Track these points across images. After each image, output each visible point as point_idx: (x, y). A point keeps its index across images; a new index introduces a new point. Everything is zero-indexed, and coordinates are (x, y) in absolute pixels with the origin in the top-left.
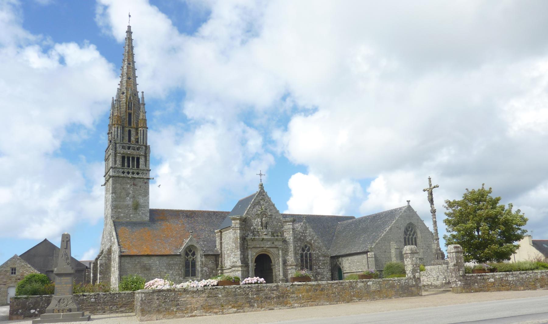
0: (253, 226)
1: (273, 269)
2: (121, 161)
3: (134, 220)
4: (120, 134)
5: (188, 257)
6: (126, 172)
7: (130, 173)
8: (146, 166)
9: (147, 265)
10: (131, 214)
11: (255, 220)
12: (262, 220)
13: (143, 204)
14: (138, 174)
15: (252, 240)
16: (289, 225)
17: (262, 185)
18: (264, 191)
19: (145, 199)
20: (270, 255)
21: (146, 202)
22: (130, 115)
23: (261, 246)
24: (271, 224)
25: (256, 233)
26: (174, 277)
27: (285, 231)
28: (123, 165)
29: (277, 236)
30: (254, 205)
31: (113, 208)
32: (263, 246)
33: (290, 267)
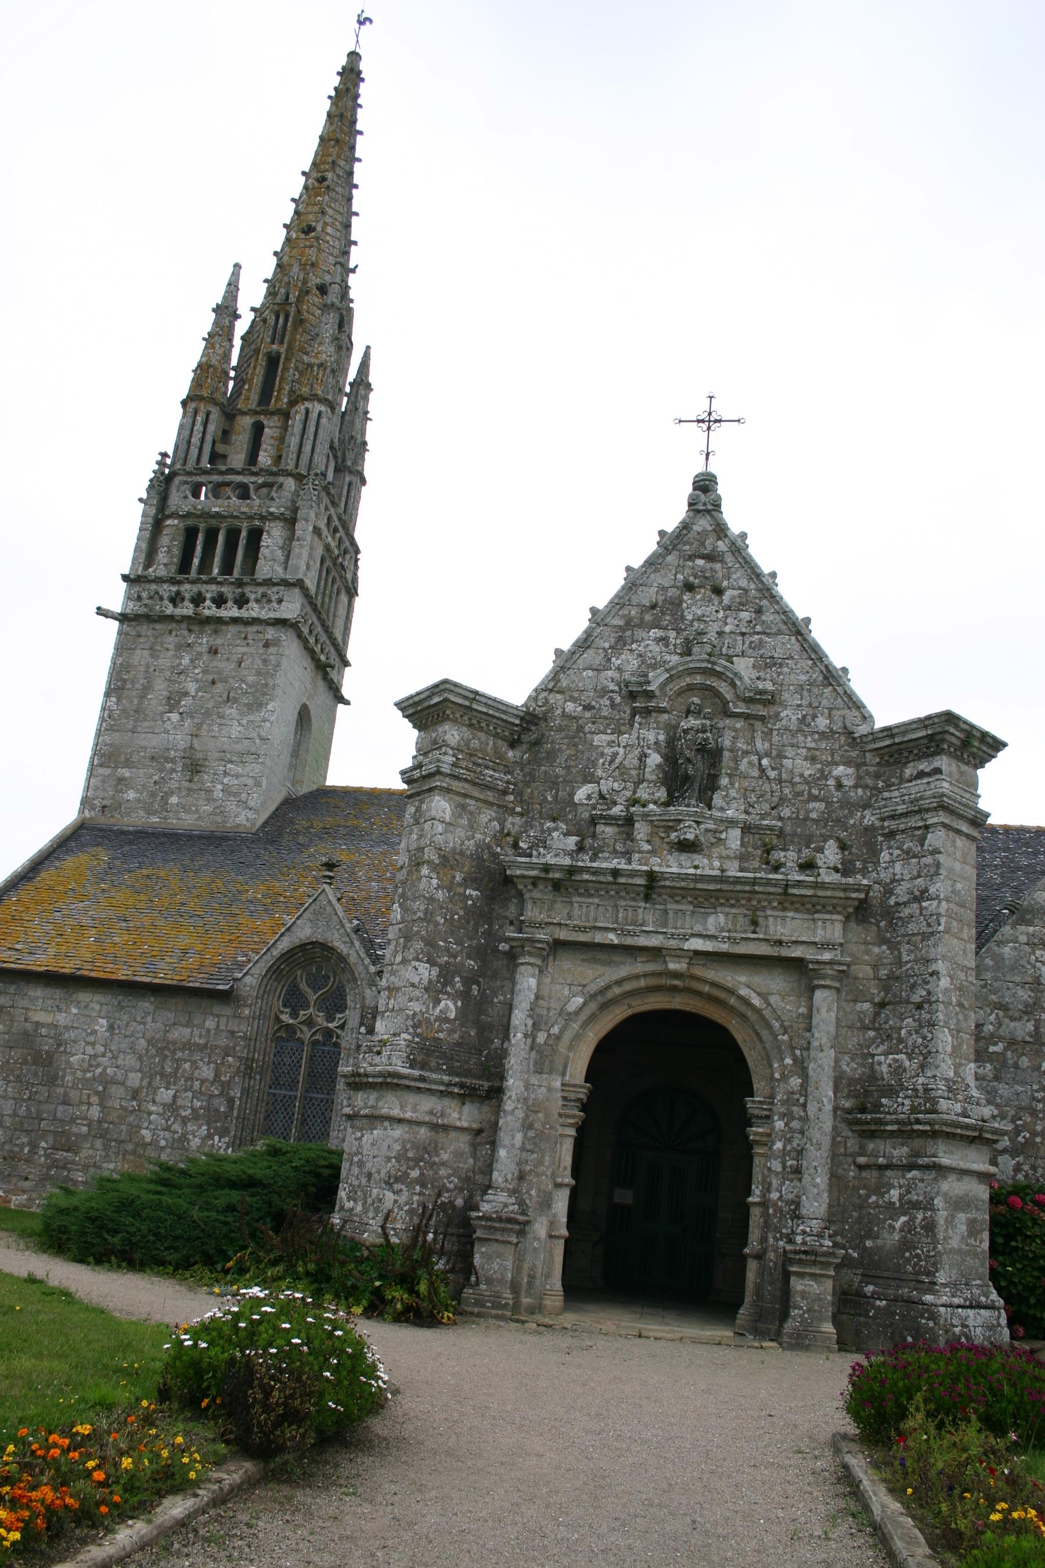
0: (589, 778)
1: (758, 1150)
2: (176, 551)
3: (185, 821)
4: (203, 440)
5: (294, 1015)
6: (187, 596)
7: (204, 600)
8: (286, 568)
9: (44, 1031)
10: (173, 793)
11: (621, 733)
12: (671, 742)
13: (238, 747)
14: (241, 602)
15: (557, 886)
16: (921, 775)
17: (705, 484)
18: (721, 530)
19: (248, 722)
20: (734, 1027)
21: (255, 735)
22: (273, 361)
23: (642, 941)
24: (756, 773)
25: (608, 831)
26: (177, 1127)
27: (891, 835)
28: (184, 566)
29: (808, 866)
30: (622, 629)
31: (96, 762)
32: (654, 941)
33: (900, 1152)
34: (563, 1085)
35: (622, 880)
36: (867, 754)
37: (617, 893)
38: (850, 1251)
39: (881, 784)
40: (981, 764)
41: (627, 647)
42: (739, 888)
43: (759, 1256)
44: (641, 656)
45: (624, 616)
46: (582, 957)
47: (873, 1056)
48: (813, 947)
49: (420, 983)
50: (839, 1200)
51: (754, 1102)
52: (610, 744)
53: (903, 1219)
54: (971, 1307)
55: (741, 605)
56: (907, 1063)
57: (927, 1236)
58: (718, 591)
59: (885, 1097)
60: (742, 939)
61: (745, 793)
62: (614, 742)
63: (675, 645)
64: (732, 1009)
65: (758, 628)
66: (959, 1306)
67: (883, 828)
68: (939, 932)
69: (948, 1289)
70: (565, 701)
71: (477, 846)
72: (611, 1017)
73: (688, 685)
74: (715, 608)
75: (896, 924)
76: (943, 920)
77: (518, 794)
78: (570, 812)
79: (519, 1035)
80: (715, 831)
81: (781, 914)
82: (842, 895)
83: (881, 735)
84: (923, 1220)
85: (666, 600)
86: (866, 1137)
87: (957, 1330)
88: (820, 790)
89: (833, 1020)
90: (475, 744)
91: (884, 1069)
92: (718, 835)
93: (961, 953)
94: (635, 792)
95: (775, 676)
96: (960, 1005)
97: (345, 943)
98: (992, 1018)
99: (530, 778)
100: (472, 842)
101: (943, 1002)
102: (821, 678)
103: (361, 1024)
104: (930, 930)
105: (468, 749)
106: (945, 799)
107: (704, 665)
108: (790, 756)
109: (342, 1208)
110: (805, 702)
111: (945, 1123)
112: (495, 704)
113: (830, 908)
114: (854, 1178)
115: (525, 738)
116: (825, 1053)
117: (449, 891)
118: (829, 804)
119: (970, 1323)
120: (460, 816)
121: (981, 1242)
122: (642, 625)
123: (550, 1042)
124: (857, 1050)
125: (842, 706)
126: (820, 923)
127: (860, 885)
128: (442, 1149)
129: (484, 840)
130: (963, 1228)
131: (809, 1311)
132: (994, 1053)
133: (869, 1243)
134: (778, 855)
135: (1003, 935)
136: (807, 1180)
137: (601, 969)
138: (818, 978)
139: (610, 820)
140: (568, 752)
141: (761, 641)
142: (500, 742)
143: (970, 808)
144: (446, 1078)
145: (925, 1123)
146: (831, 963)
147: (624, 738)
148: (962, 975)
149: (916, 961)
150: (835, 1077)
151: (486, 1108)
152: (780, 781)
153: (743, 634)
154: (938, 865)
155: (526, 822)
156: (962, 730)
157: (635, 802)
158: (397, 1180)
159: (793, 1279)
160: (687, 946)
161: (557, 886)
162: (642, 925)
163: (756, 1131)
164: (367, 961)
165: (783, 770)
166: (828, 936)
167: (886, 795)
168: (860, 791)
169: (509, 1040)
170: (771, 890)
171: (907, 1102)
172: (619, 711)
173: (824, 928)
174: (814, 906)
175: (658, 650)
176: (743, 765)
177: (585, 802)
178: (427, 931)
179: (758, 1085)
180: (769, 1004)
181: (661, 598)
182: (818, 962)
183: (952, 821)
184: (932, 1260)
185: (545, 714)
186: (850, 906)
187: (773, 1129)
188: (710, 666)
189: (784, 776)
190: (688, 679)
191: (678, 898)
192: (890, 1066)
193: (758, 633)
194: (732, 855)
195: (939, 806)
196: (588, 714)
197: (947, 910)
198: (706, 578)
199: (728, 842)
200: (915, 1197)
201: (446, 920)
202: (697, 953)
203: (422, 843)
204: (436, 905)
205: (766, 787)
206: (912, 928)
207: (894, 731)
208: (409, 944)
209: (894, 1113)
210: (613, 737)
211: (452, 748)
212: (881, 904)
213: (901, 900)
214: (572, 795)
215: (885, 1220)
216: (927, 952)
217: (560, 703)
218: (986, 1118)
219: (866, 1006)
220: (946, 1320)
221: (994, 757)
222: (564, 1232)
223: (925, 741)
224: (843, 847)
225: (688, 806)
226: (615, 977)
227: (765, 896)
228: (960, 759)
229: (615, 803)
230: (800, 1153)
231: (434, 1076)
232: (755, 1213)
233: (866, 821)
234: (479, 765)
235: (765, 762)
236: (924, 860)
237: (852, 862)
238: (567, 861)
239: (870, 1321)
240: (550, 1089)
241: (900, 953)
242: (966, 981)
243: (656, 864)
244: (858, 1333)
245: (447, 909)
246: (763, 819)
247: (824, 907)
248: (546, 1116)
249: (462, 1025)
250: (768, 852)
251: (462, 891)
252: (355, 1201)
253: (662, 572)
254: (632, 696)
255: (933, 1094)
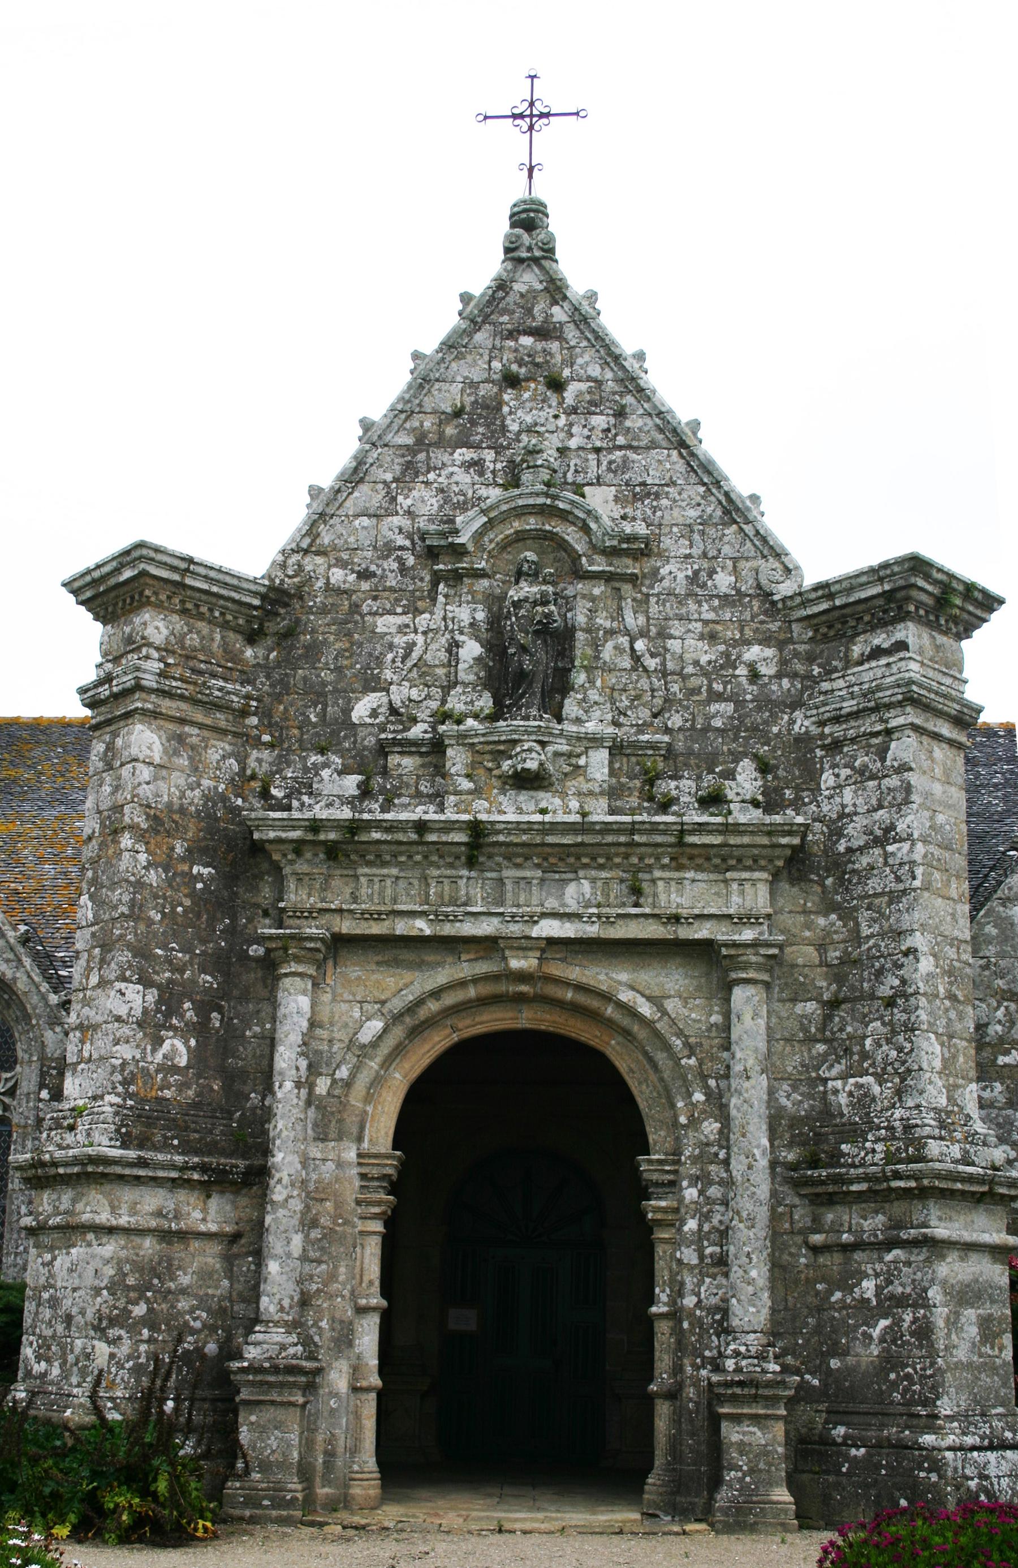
0: (372, 684)
11: (417, 612)
12: (495, 622)
16: (877, 653)
20: (614, 1050)
23: (468, 929)
24: (626, 663)
25: (406, 763)
27: (835, 746)
29: (713, 800)
30: (411, 450)
32: (486, 928)
34: (360, 1155)
35: (432, 837)
36: (794, 626)
37: (426, 857)
38: (807, 1377)
39: (816, 671)
40: (966, 631)
41: (421, 478)
42: (610, 839)
43: (673, 1395)
44: (442, 491)
45: (414, 429)
46: (380, 958)
47: (825, 1080)
48: (727, 922)
49: (129, 1015)
50: (786, 1301)
51: (650, 1162)
52: (402, 629)
53: (883, 1323)
54: (991, 1448)
55: (592, 405)
56: (876, 1089)
57: (921, 1347)
58: (557, 385)
59: (846, 1142)
60: (619, 916)
61: (612, 693)
62: (407, 626)
63: (493, 472)
64: (609, 1024)
65: (621, 440)
66: (973, 1448)
67: (822, 736)
68: (914, 890)
69: (956, 1424)
70: (330, 567)
71: (206, 797)
72: (427, 1047)
73: (517, 532)
74: (553, 412)
75: (850, 881)
76: (919, 871)
77: (265, 714)
78: (346, 737)
79: (289, 1085)
80: (570, 755)
81: (676, 875)
82: (765, 841)
83: (813, 595)
84: (913, 1323)
85: (476, 402)
86: (822, 1204)
87: (973, 1484)
88: (725, 684)
89: (763, 1030)
90: (193, 640)
91: (843, 1099)
92: (574, 761)
93: (949, 918)
94: (444, 702)
95: (649, 512)
96: (952, 997)
97: (7, 961)
98: (1000, 1014)
99: (283, 688)
100: (197, 792)
101: (925, 994)
102: (719, 513)
103: (42, 1086)
104: (901, 887)
105: (183, 648)
106: (914, 688)
107: (540, 500)
108: (677, 633)
109: (28, 1374)
110: (696, 551)
111: (938, 1176)
112: (221, 577)
113: (749, 862)
114: (807, 1266)
115: (271, 627)
116: (752, 1081)
117: (166, 871)
118: (739, 704)
119: (992, 1471)
120: (176, 753)
121: (1001, 1350)
122: (442, 442)
123: (337, 1092)
124: (800, 1073)
125: (752, 554)
126: (735, 886)
127: (792, 825)
128: (179, 1268)
129: (216, 788)
130: (974, 1330)
131: (751, 1471)
132: (1005, 1065)
133: (834, 1363)
134: (667, 786)
135: (1010, 889)
136: (736, 1272)
137: (408, 976)
138: (736, 969)
139: (409, 747)
140: (338, 645)
141: (625, 460)
142: (231, 635)
143: (953, 700)
144: (179, 1159)
145: (908, 1178)
146: (755, 944)
147: (423, 620)
148: (951, 953)
149: (882, 935)
150: (771, 1117)
151: (243, 1201)
152: (664, 673)
153: (597, 450)
154: (908, 789)
155: (280, 756)
156: (936, 582)
157: (444, 716)
158: (113, 1322)
159: (724, 1425)
160: (536, 932)
161: (332, 852)
162: (465, 904)
163: (657, 1205)
164: (45, 987)
165: (668, 656)
166: (748, 904)
167: (825, 686)
168: (786, 683)
169: (273, 1094)
170: (659, 839)
171: (880, 1147)
172: (413, 579)
173: (742, 893)
174: (724, 860)
175: (468, 480)
176: (607, 652)
177: (368, 720)
178: (136, 935)
179: (655, 1135)
180: (664, 1013)
181: (468, 400)
182: (735, 945)
183: (927, 720)
184: (930, 1382)
185: (299, 587)
186: (778, 858)
187: (681, 1200)
188: (549, 501)
189: (670, 665)
190: (516, 524)
191: (519, 860)
192: (850, 1094)
193: (620, 448)
194: (597, 790)
195: (905, 699)
196: (365, 586)
197: (925, 856)
198: (537, 365)
199: (589, 770)
200: (900, 1290)
201: (164, 914)
202: (552, 942)
203: (120, 798)
204: (146, 893)
205: (644, 683)
206: (874, 885)
207: (833, 589)
208: (109, 956)
209: (862, 1165)
210: (406, 619)
211: (158, 649)
212: (825, 852)
213: (856, 844)
214: (347, 711)
215: (857, 1327)
216: (898, 921)
217: (321, 570)
218: (998, 1164)
219: (811, 1007)
220: (956, 1469)
221: (985, 621)
222: (375, 1381)
223: (881, 602)
224: (764, 768)
225: (526, 718)
226: (430, 985)
227: (649, 850)
228: (933, 626)
229: (414, 720)
230: (724, 1234)
231: (160, 1157)
232: (663, 1329)
233: (796, 728)
234: (201, 673)
235: (640, 645)
236: (886, 782)
237: (778, 791)
238: (346, 813)
239: (844, 1480)
240: (340, 1164)
241: (857, 924)
242: (959, 960)
243: (482, 811)
244: (826, 1498)
245: (165, 898)
246: (641, 731)
247: (739, 860)
248: (338, 1206)
249: (199, 1076)
250: (651, 782)
251: (186, 868)
252: (48, 1360)
253: (469, 358)
254: (432, 554)
255: (918, 1132)
